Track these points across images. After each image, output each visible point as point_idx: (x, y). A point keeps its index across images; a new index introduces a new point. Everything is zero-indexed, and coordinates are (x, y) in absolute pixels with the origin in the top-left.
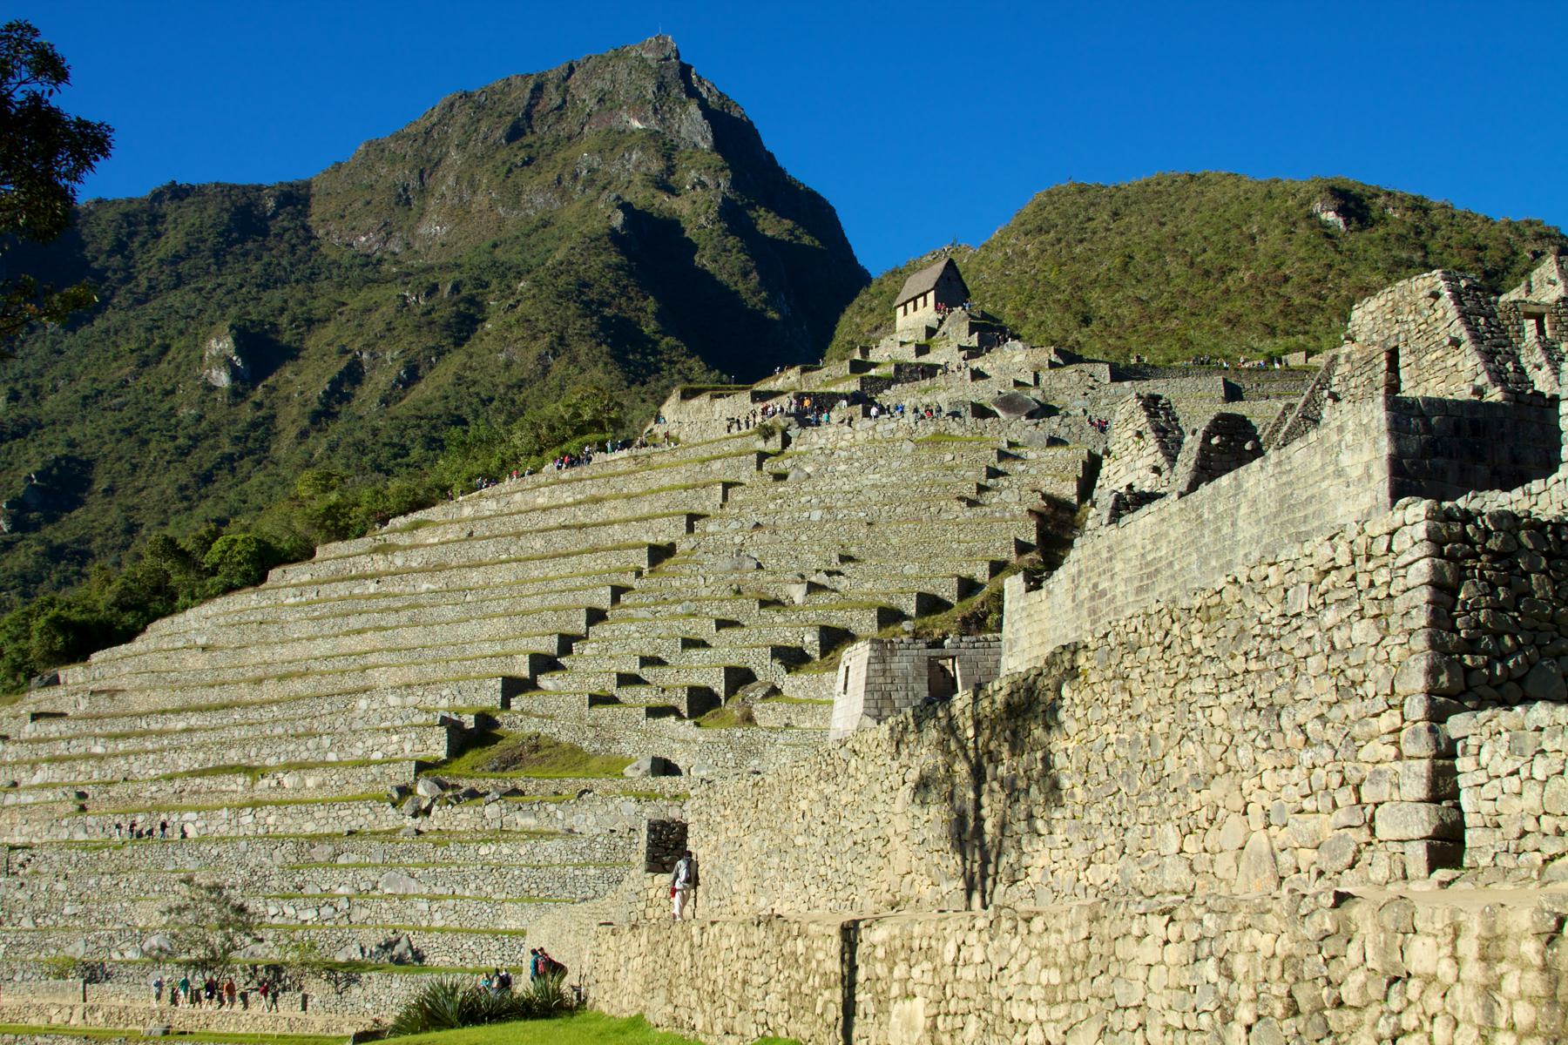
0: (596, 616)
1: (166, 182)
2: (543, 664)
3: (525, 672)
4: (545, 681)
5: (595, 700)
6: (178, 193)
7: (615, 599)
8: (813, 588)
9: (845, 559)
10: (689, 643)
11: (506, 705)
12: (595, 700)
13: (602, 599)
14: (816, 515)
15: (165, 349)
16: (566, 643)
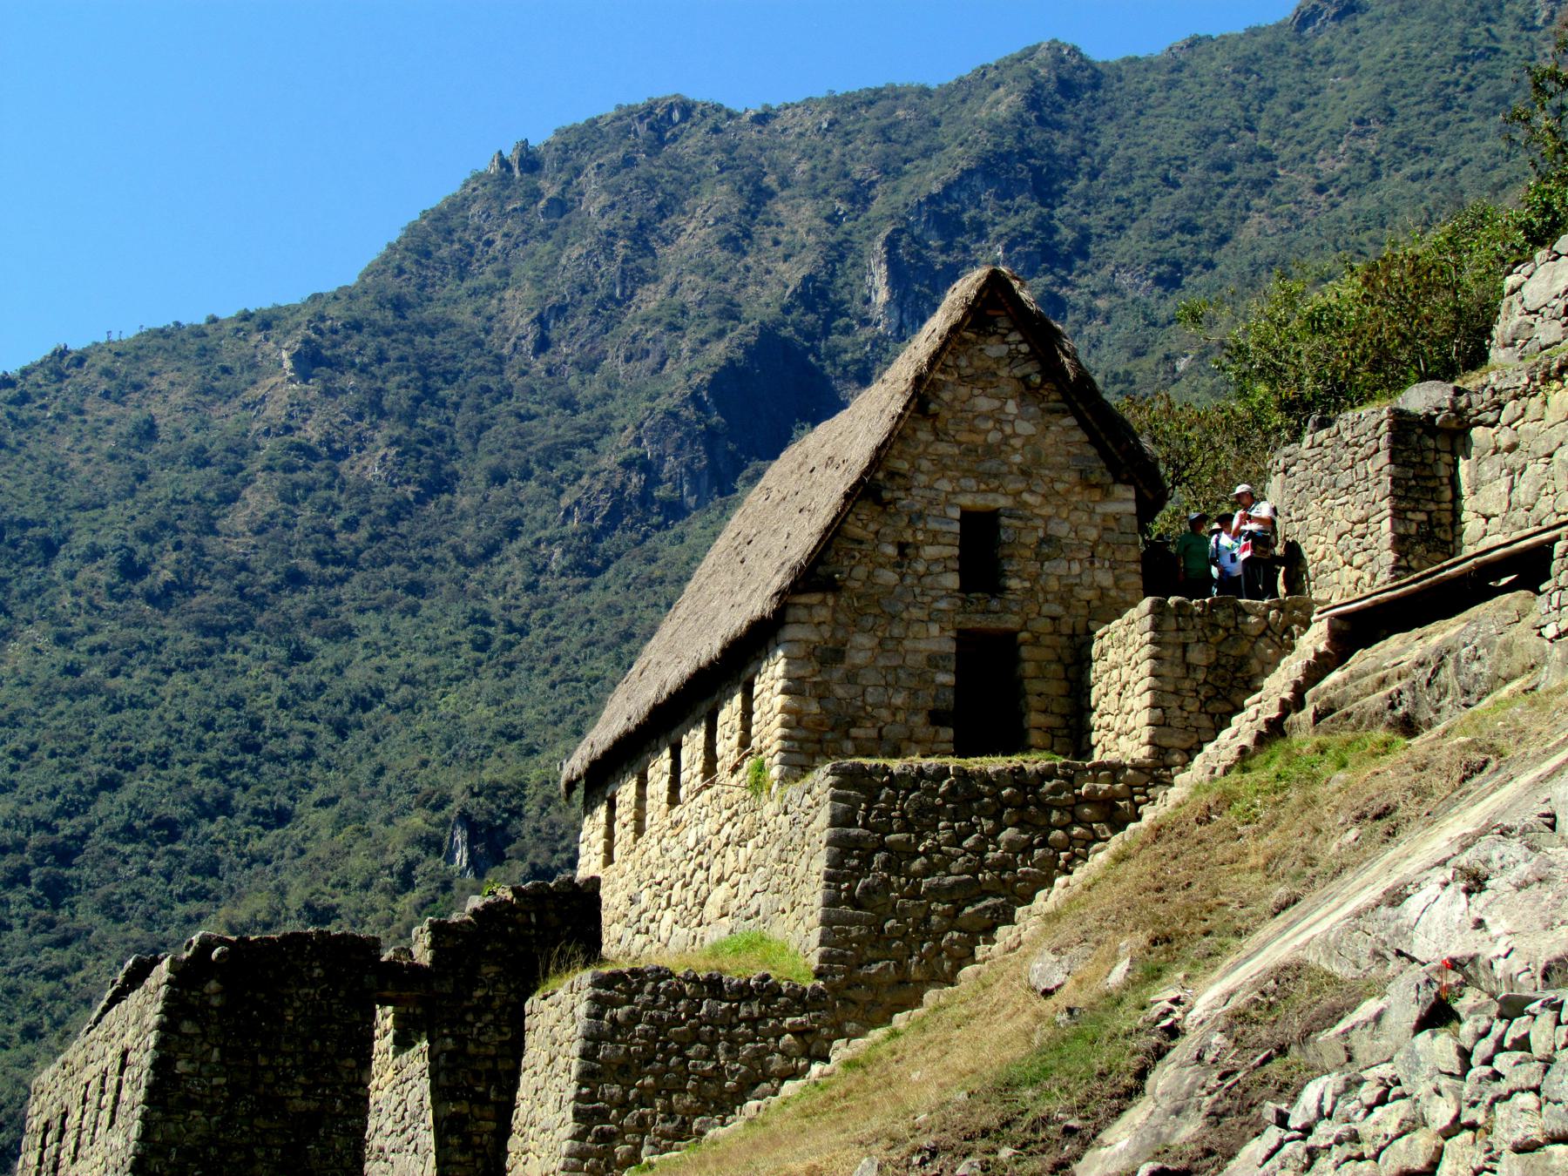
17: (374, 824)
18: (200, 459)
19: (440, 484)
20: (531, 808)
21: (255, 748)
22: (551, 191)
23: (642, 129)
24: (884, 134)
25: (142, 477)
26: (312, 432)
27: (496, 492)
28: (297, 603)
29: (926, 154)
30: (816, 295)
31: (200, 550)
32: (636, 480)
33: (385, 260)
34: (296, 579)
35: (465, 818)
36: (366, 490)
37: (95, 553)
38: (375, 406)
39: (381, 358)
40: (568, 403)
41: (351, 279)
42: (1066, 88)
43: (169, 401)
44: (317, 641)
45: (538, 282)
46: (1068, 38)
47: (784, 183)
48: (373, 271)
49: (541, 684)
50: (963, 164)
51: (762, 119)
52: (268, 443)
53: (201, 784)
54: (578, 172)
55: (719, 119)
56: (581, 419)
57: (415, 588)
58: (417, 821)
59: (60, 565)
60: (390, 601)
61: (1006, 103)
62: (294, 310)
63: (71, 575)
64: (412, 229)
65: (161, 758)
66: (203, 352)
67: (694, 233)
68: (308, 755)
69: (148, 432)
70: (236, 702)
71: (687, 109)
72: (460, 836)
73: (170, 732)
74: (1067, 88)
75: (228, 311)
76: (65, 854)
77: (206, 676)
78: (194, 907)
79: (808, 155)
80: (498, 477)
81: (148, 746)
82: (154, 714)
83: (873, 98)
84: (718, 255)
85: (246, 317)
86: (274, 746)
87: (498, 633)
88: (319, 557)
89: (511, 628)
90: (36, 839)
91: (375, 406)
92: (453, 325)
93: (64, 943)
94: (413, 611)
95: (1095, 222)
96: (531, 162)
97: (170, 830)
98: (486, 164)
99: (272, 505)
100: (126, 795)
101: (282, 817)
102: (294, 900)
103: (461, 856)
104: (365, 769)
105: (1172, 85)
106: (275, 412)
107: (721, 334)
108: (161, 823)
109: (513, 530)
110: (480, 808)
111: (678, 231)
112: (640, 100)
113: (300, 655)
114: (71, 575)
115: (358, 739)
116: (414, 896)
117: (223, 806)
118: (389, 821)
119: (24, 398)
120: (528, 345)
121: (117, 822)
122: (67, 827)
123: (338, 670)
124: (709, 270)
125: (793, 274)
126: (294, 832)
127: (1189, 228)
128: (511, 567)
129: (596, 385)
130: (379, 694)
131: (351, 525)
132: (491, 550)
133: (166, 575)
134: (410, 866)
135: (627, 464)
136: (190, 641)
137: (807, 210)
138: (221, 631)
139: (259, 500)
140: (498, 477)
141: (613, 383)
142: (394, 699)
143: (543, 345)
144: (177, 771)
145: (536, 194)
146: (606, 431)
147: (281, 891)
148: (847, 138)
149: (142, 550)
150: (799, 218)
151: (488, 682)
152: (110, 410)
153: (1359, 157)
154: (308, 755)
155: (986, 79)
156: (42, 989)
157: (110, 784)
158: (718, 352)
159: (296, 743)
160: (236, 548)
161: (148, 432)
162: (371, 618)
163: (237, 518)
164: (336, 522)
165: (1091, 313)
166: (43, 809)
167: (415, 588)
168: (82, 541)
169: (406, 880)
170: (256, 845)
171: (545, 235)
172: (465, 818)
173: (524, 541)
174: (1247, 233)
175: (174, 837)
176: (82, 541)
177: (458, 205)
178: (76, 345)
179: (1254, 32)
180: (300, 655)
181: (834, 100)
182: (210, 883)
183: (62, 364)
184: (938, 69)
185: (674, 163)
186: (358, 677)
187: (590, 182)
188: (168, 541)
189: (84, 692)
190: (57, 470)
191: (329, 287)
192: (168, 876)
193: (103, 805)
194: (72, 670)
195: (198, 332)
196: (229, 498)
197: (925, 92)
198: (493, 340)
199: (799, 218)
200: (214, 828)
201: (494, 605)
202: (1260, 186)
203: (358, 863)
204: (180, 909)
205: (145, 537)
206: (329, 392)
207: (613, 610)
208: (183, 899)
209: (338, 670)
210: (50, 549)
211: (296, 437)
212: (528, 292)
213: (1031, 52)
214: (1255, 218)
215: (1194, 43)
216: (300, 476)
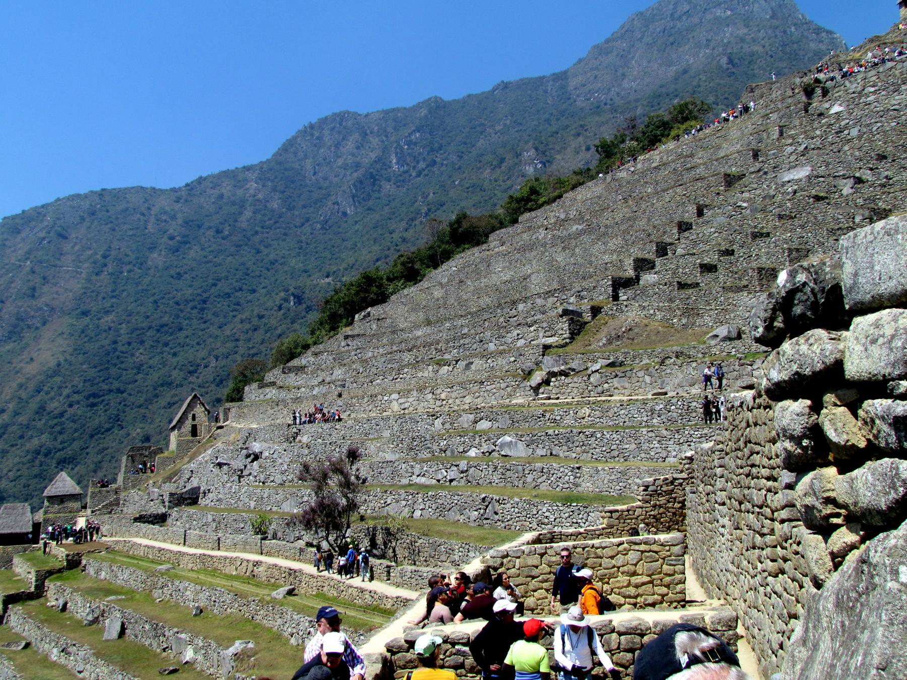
0: (684, 227)
1: (497, 81)
2: (643, 265)
3: (631, 273)
4: (648, 278)
5: (682, 286)
6: (505, 86)
7: (700, 213)
8: (859, 181)
9: (882, 157)
10: (756, 236)
11: (616, 298)
12: (682, 286)
13: (690, 212)
14: (854, 132)
15: (502, 160)
16: (662, 250)
17: (273, 294)
18: (234, 203)
19: (291, 208)
20: (307, 292)
21: (248, 275)
22: (317, 134)
23: (338, 119)
24: (395, 120)
25: (220, 208)
26: (260, 196)
27: (304, 210)
28: (257, 238)
29: (405, 125)
30: (378, 160)
31: (234, 226)
32: (336, 207)
33: (277, 152)
34: (257, 233)
35: (293, 294)
36: (273, 210)
37: (210, 228)
38: (274, 190)
39: (276, 178)
40: (320, 188)
41: (269, 156)
42: (437, 107)
43: (226, 189)
44: (262, 248)
45: (313, 158)
46: (439, 95)
47: (371, 133)
48: (274, 155)
49: (313, 258)
50: (413, 128)
51: (366, 116)
52: (250, 199)
53: (235, 284)
54: (323, 129)
55: (356, 115)
56: (324, 192)
57: (285, 234)
58: (282, 294)
59: (202, 231)
60: (279, 238)
61: (423, 112)
62: (256, 165)
63: (204, 234)
64: (284, 145)
65: (227, 278)
66: (234, 177)
67: (350, 145)
68: (260, 276)
69: (221, 196)
70: (243, 264)
71: (349, 113)
72: (292, 298)
73: (229, 272)
74: (438, 107)
75: (240, 166)
76: (205, 302)
77: (237, 257)
78: (234, 313)
79: (377, 125)
80: (304, 207)
81: (223, 275)
82: (224, 267)
83: (393, 110)
84: (355, 150)
85: (244, 167)
86: (252, 274)
87: (304, 245)
88: (263, 227)
89: (307, 244)
90: (198, 298)
91: (274, 190)
92: (293, 169)
93: (205, 322)
94: (284, 240)
95: (444, 142)
96: (312, 127)
97: (228, 295)
98: (301, 127)
99: (251, 214)
100: (218, 288)
101: (254, 291)
102: (255, 313)
103: (292, 303)
104: (273, 279)
105: (463, 107)
106: (252, 192)
107: (356, 171)
108: (226, 294)
109: (308, 220)
110: (297, 292)
111: (347, 145)
112: (337, 111)
113: (258, 252)
114: (204, 234)
115: (273, 271)
116: (282, 312)
117: (241, 289)
118: (277, 294)
119: (192, 189)
120: (312, 173)
121: (216, 294)
122: (205, 295)
123: (267, 255)
124: (353, 155)
125: (373, 156)
126: (257, 295)
127: (465, 143)
128: (307, 229)
129: (327, 184)
130: (276, 261)
131: (270, 219)
132: (303, 225)
133: (227, 233)
134: (281, 305)
135: (334, 204)
136: (233, 249)
137: (377, 140)
138: (240, 246)
139: (248, 214)
140: (304, 207)
141: (331, 183)
142: (280, 262)
143: (315, 174)
144: (230, 281)
145: (312, 135)
146: (329, 195)
147: (253, 311)
148: (386, 121)
149: (221, 227)
150: (375, 141)
151: (302, 258)
152: (212, 191)
153: (505, 125)
154: (260, 276)
155: (419, 106)
156: (200, 333)
157: (215, 285)
158: (355, 175)
159: (257, 273)
160: (244, 225)
161: (221, 196)
162: (275, 243)
163: (243, 218)
164: (266, 219)
165: (442, 164)
166: (199, 291)
167: (285, 234)
168: (207, 225)
169: (280, 308)
170: (249, 298)
171: (315, 146)
172: (293, 294)
173: (310, 222)
174: (479, 144)
175: (229, 297)
176: (207, 225)
177: (294, 138)
178: (204, 175)
179: (483, 93)
180: (258, 252)
181: (383, 111)
182: (238, 307)
183: (201, 180)
184: (409, 103)
185: (345, 128)
186: (272, 257)
187: (326, 132)
188: (227, 225)
189: (208, 262)
190: (201, 207)
191: (264, 160)
192: (229, 306)
193: (213, 290)
194: (205, 257)
195: (233, 171)
196: (241, 213)
197: (405, 109)
198: (303, 172)
199: (375, 141)
200: (238, 294)
201: (303, 238)
202: (481, 133)
203: (270, 304)
204: (232, 314)
205: (221, 223)
206: (263, 186)
207: (330, 239)
208: (232, 311)
209: (267, 255)
210: (199, 227)
211: (256, 198)
212: (311, 160)
213: (429, 99)
214: (481, 141)
215: (469, 96)
216: (257, 207)
